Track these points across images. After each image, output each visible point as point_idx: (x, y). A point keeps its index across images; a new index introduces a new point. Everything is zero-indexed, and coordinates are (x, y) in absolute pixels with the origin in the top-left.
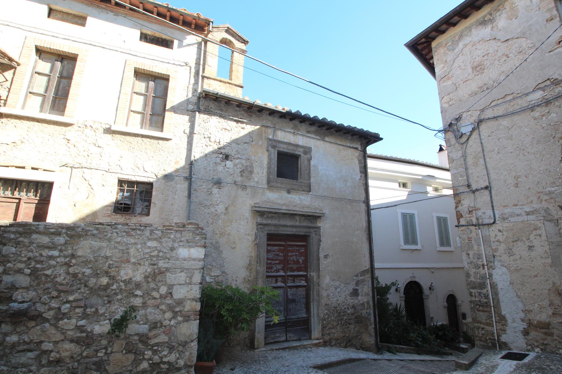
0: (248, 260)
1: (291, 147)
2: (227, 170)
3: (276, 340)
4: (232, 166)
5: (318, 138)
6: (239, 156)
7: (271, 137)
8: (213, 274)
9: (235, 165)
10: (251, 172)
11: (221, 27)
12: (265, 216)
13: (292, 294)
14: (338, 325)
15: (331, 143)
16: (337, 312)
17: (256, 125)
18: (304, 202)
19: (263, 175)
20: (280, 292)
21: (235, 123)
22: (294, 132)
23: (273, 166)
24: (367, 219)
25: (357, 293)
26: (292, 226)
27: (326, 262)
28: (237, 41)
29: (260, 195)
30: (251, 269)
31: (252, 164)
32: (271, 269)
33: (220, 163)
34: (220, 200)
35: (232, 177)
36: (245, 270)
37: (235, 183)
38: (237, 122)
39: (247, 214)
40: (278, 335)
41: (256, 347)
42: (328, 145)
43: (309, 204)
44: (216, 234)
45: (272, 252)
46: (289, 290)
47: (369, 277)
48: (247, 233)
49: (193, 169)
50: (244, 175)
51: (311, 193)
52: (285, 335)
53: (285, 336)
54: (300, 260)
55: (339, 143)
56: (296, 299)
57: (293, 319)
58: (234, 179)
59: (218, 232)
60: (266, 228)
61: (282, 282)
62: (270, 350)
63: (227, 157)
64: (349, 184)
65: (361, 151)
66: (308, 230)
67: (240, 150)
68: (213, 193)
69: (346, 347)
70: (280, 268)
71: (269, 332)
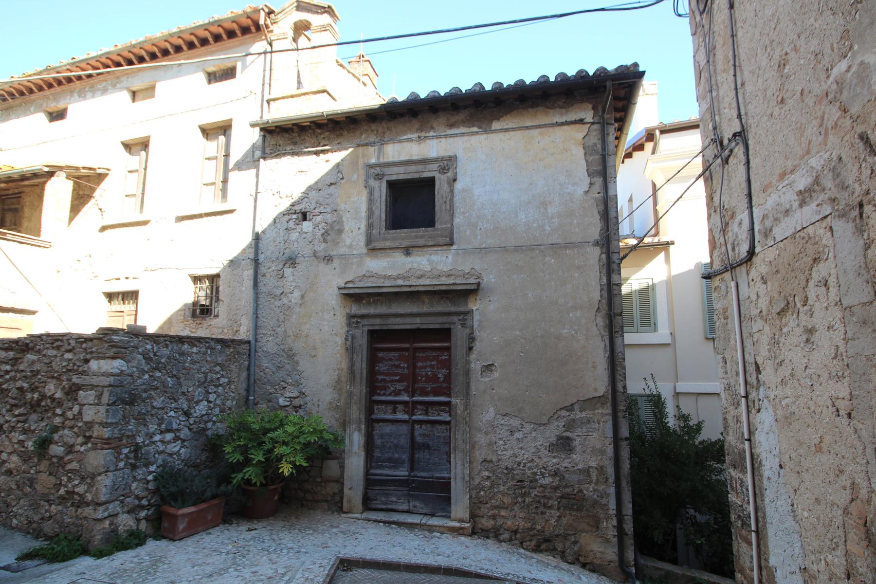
0: (336, 374)
1: (413, 168)
2: (304, 235)
3: (390, 507)
4: (311, 229)
5: (475, 129)
6: (322, 209)
7: (373, 161)
8: (288, 394)
9: (316, 226)
10: (340, 231)
11: (286, 6)
12: (364, 301)
13: (424, 435)
14: (516, 504)
15: (506, 130)
16: (513, 478)
17: (346, 149)
18: (440, 267)
19: (360, 232)
20: (404, 429)
21: (314, 156)
22: (419, 137)
23: (377, 213)
24: (605, 281)
25: (569, 445)
26: (411, 315)
27: (487, 379)
28: (316, 16)
29: (354, 267)
30: (340, 390)
31: (341, 218)
32: (385, 390)
33: (294, 227)
34: (294, 284)
35: (311, 245)
36: (331, 390)
37: (315, 254)
38: (317, 153)
39: (333, 302)
40: (394, 499)
41: (345, 509)
42: (501, 135)
43: (450, 268)
44: (289, 337)
45: (386, 360)
46: (417, 426)
47: (607, 414)
48: (334, 332)
49: (260, 245)
50: (329, 238)
51: (455, 247)
52: (406, 501)
53: (407, 504)
54: (440, 376)
55: (529, 124)
56: (430, 443)
57: (421, 477)
58: (315, 248)
59: (291, 334)
60: (365, 322)
61: (406, 413)
62: (364, 519)
63: (304, 216)
64: (552, 210)
65: (593, 123)
66: (445, 319)
67: (321, 200)
68: (285, 275)
69: (537, 549)
70: (401, 388)
71: (377, 492)
